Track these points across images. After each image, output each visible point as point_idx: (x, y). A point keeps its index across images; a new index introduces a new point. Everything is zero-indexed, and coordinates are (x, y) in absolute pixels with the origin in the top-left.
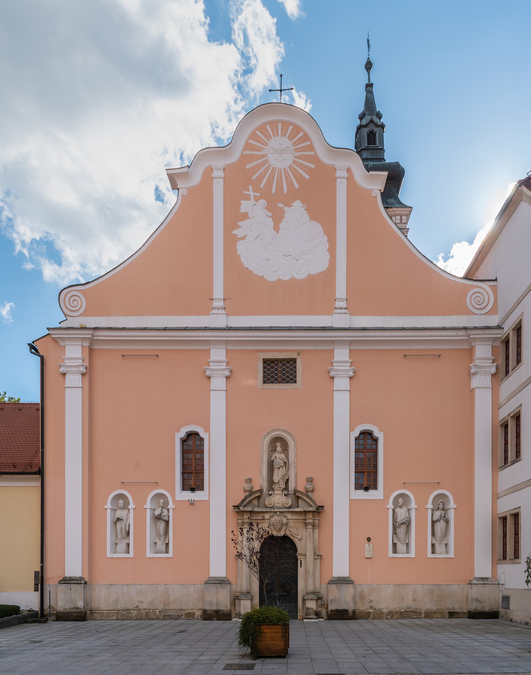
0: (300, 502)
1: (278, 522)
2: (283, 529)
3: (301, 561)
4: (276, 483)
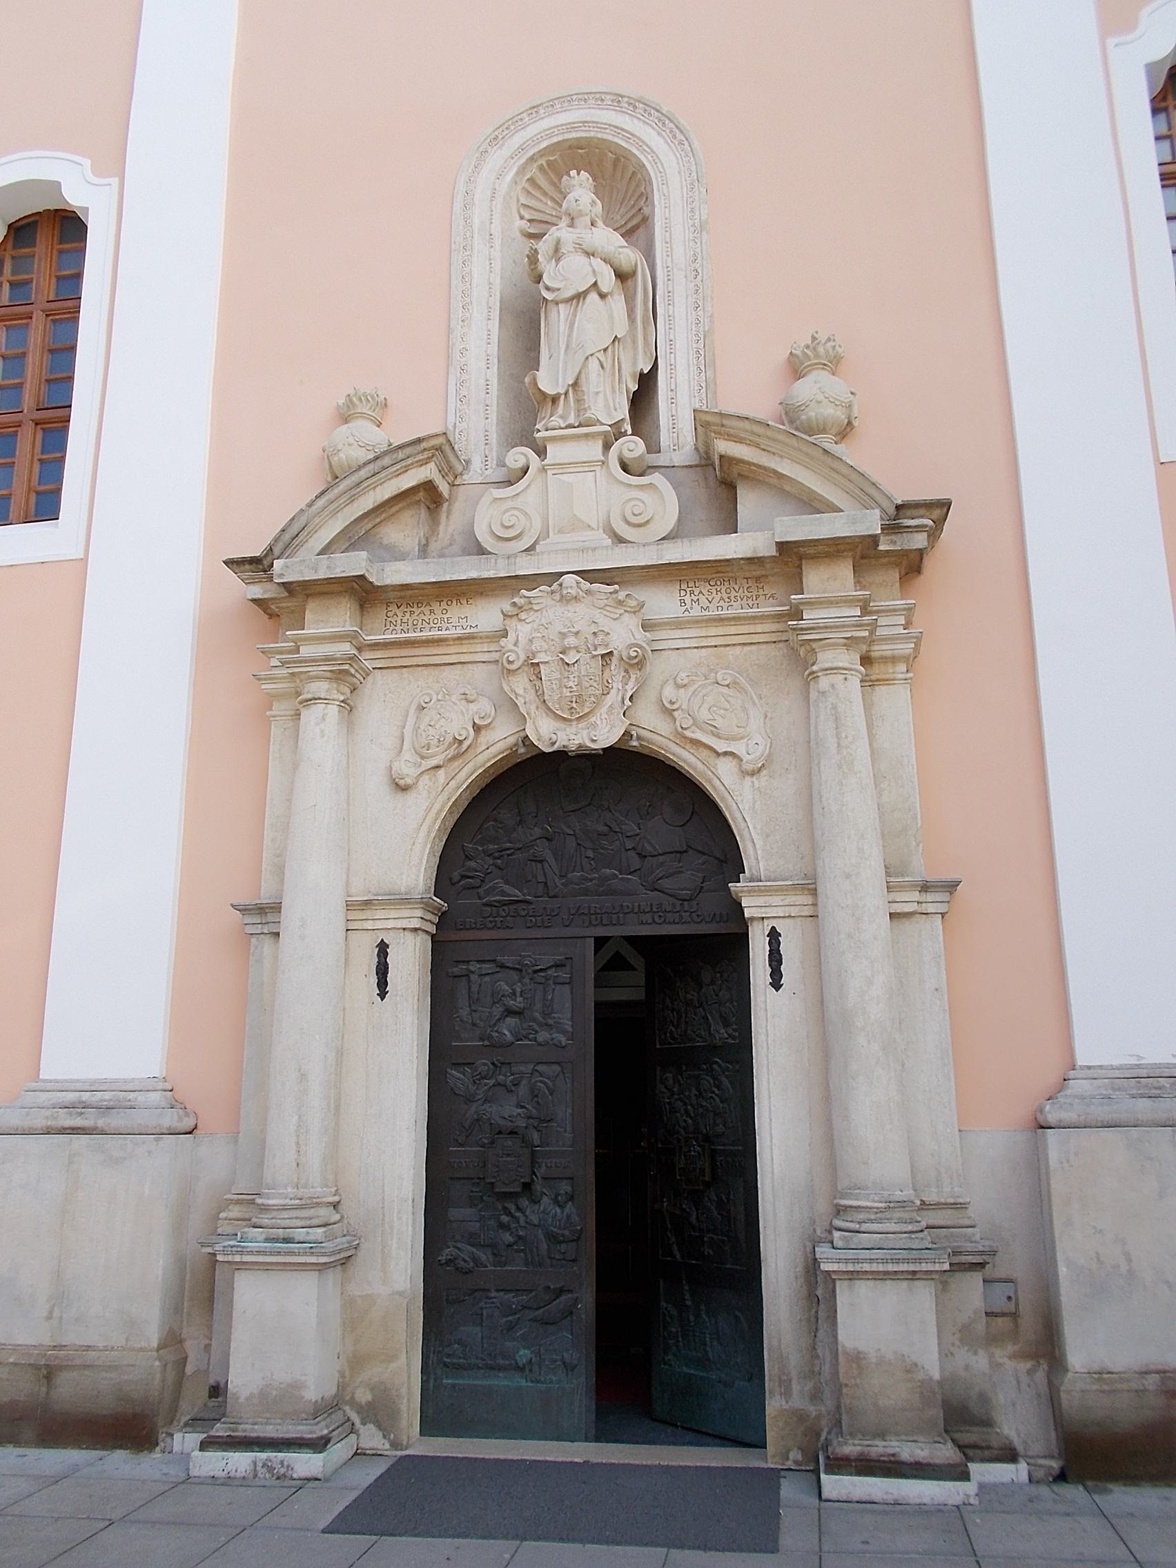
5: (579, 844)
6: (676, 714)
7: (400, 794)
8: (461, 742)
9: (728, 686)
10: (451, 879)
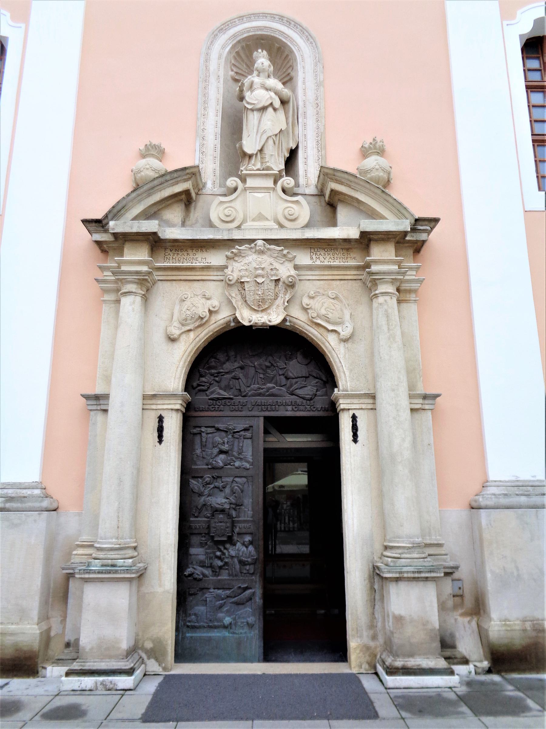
0: (342, 213)
1: (260, 272)
2: (279, 301)
3: (354, 418)
4: (250, 156)
5: (256, 371)
6: (309, 311)
7: (170, 344)
8: (202, 318)
9: (333, 299)
10: (192, 386)
